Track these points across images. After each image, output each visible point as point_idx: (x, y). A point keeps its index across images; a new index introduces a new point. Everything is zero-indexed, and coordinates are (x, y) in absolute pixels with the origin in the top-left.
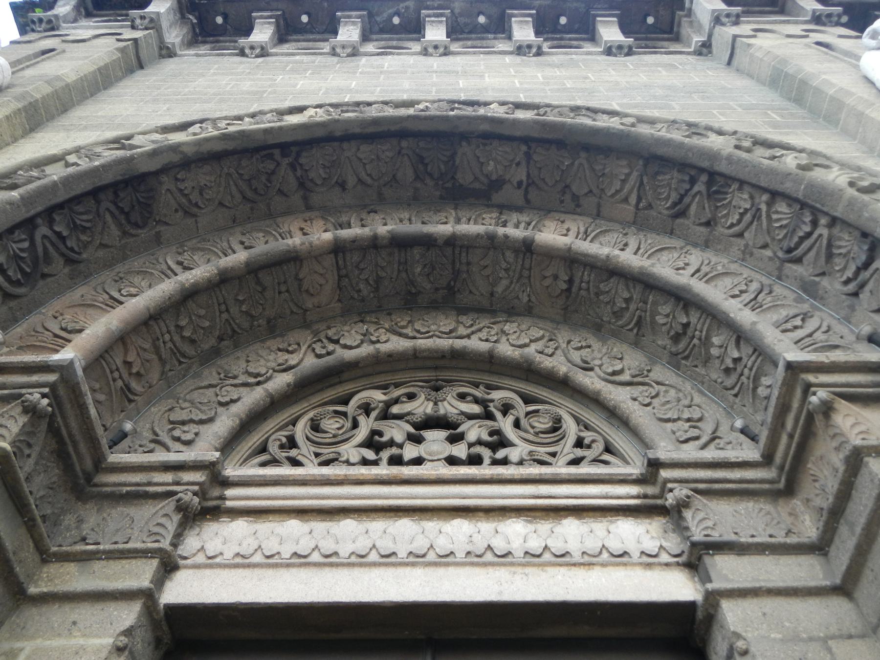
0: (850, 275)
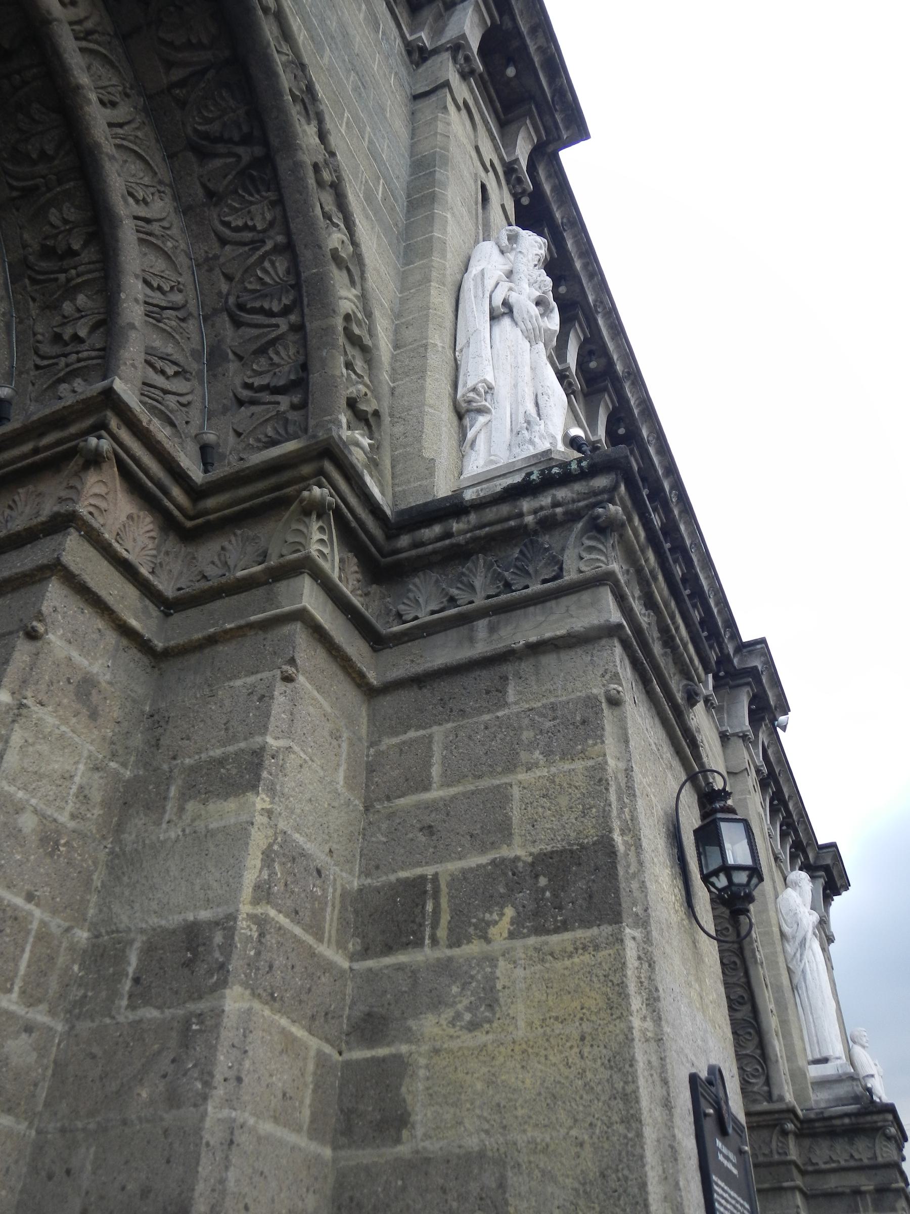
0: (256, 384)
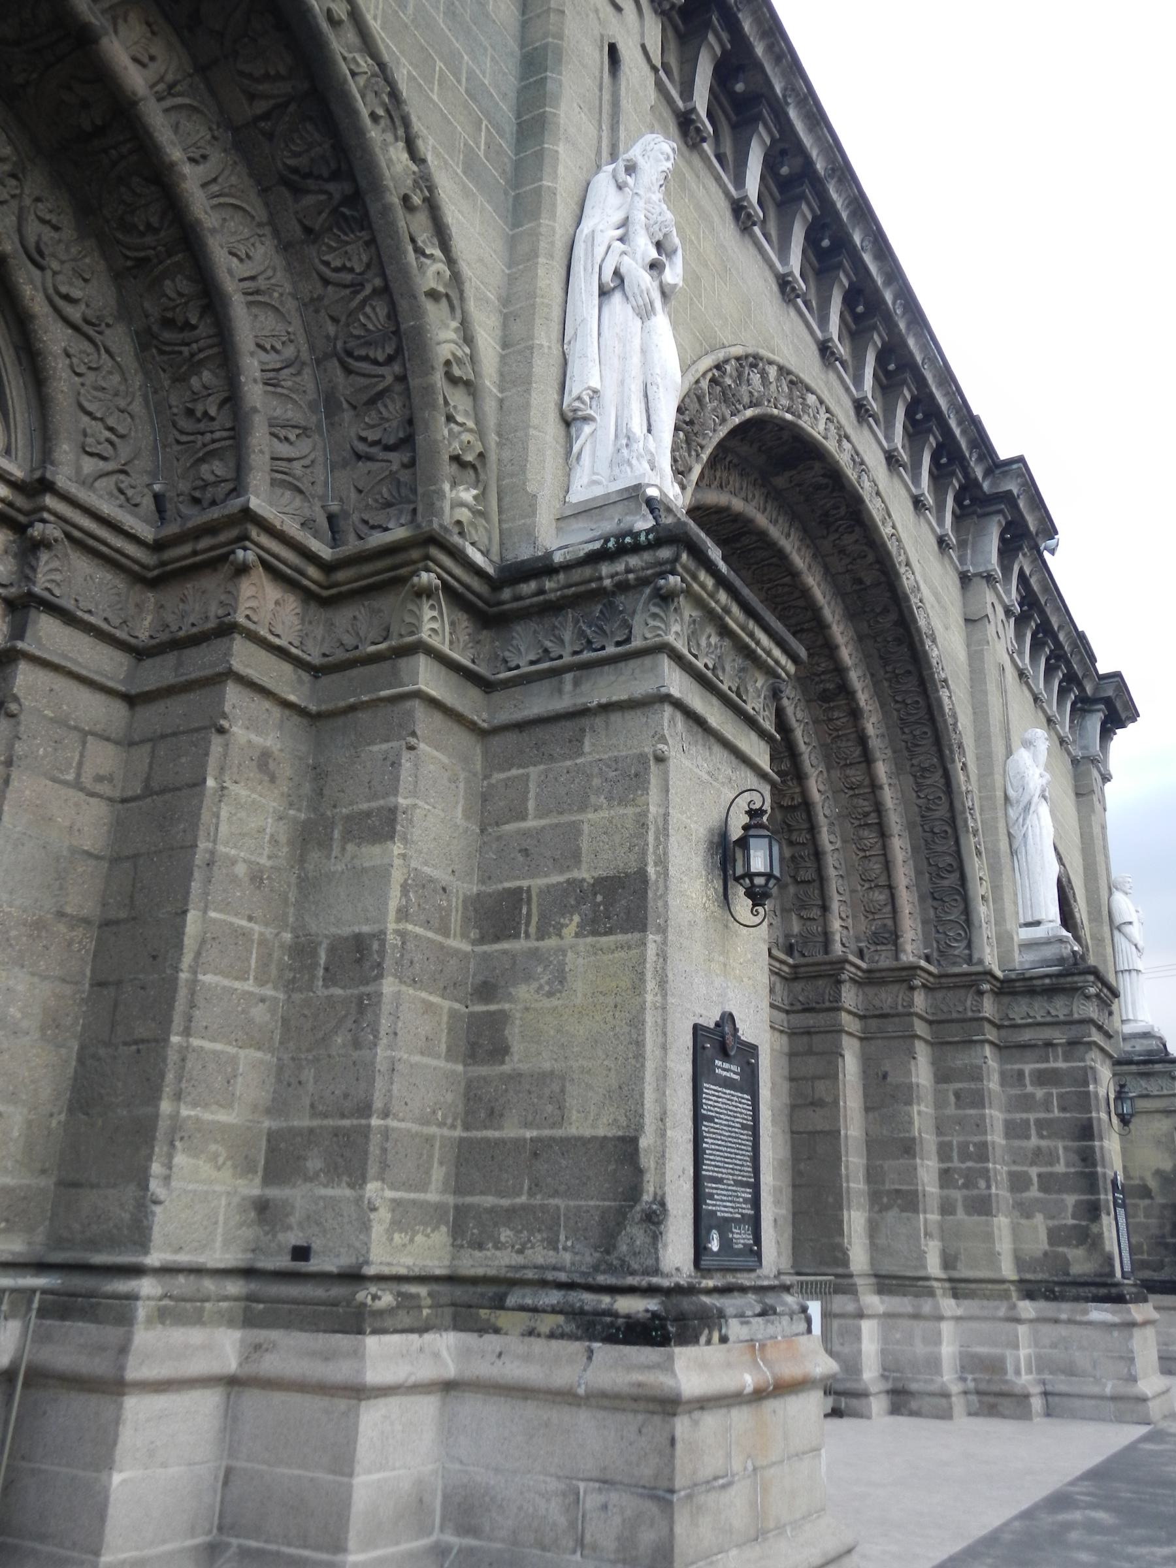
0: (370, 439)
